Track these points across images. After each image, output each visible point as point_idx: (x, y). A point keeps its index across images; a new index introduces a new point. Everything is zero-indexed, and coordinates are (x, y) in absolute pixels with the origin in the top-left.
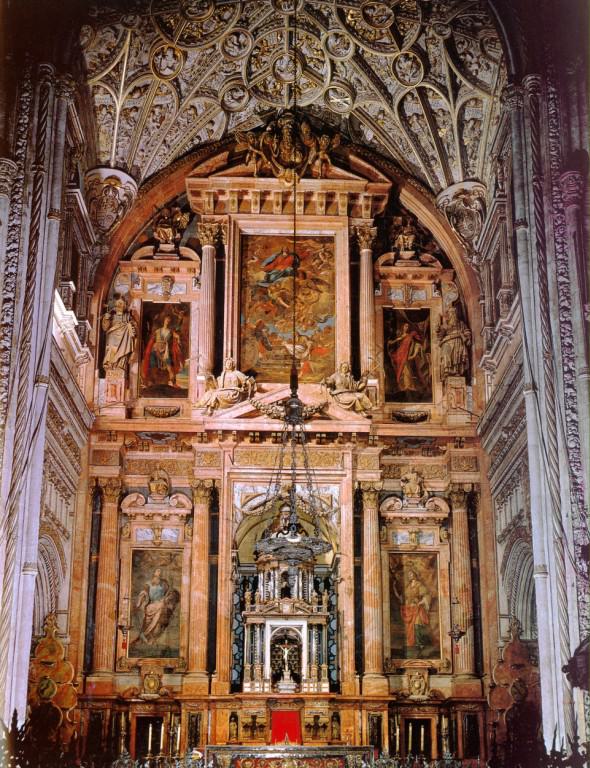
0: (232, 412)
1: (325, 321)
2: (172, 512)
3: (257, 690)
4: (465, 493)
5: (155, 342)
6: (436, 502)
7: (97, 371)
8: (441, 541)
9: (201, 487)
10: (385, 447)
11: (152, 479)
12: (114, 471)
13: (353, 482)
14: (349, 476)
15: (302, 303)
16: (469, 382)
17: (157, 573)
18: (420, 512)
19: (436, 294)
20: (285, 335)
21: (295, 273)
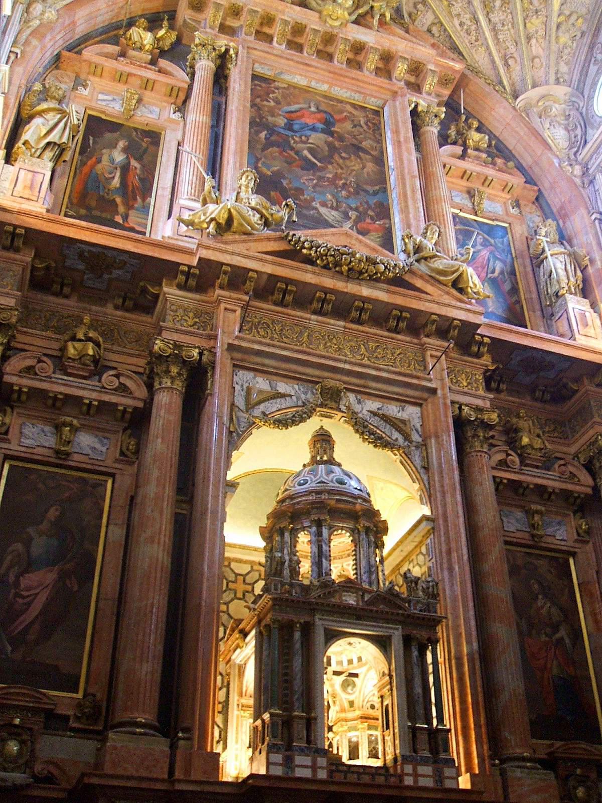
0: (252, 244)
2: (106, 398)
3: (300, 773)
5: (99, 161)
6: (571, 468)
8: (578, 534)
9: (177, 356)
11: (74, 339)
15: (338, 164)
17: (53, 513)
18: (551, 481)
19: (514, 211)
20: (316, 196)
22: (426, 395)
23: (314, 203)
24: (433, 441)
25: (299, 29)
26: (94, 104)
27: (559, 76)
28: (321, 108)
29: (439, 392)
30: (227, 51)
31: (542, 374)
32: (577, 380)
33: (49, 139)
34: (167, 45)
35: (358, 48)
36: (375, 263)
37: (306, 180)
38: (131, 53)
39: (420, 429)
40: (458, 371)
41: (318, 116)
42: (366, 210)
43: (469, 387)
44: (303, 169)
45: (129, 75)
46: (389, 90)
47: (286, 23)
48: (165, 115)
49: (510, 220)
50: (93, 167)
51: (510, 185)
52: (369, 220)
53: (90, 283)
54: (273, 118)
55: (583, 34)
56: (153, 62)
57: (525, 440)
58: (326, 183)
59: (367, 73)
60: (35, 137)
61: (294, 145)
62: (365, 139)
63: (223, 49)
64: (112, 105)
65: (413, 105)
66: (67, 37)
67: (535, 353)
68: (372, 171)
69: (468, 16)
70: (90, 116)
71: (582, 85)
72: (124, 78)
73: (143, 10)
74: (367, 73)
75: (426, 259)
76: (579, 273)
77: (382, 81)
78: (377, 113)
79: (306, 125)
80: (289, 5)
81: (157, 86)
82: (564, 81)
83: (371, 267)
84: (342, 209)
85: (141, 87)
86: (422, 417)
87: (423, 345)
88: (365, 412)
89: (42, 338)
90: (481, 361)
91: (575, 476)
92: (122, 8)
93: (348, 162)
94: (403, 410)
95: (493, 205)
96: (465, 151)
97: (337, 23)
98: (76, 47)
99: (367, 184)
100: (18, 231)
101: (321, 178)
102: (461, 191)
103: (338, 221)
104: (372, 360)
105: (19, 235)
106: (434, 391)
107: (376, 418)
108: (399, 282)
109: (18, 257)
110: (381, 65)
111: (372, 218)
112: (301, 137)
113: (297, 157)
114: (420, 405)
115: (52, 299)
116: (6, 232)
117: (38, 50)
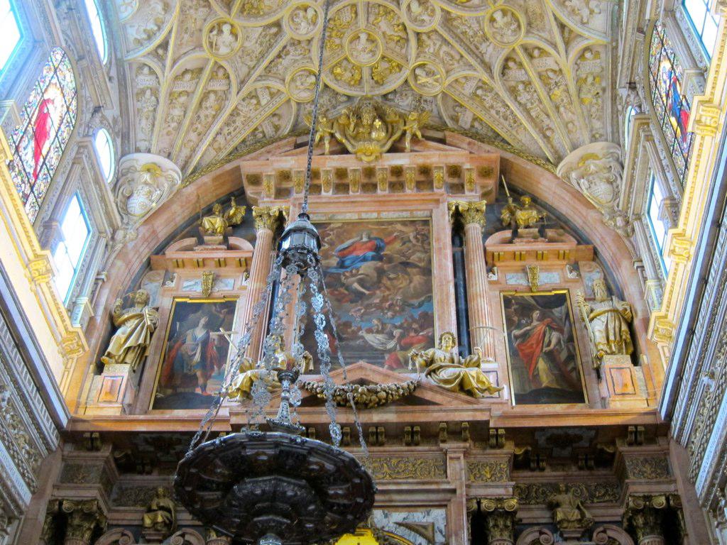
1: (420, 305)
4: (657, 511)
5: (184, 343)
6: (610, 533)
7: (92, 367)
10: (519, 452)
11: (150, 510)
12: (90, 492)
13: (469, 500)
14: (462, 491)
16: (635, 360)
20: (363, 324)
21: (380, 258)
22: (449, 496)
23: (360, 333)
24: (454, 538)
25: (341, 173)
26: (180, 293)
27: (594, 132)
28: (372, 236)
29: (458, 492)
30: (281, 213)
31: (574, 445)
32: (613, 443)
33: (128, 345)
34: (238, 219)
35: (397, 171)
36: (377, 392)
37: (355, 312)
38: (206, 238)
39: (443, 530)
40: (482, 465)
41: (369, 245)
42: (410, 325)
43: (493, 478)
44: (352, 302)
45: (204, 260)
46: (431, 200)
47: (327, 172)
48: (238, 285)
49: (567, 285)
50: (178, 350)
51: (562, 252)
52: (412, 334)
53: (163, 459)
54: (327, 261)
55: (604, 90)
56: (225, 241)
57: (560, 516)
58: (373, 309)
59: (410, 191)
60: (116, 346)
61: (345, 281)
62: (414, 253)
63: (277, 214)
64: (195, 288)
65: (454, 208)
66: (152, 245)
67: (555, 431)
68: (419, 283)
69: (500, 105)
70: (178, 304)
71: (616, 135)
72: (201, 264)
73: (217, 196)
74: (410, 191)
75: (434, 371)
76: (624, 327)
77: (426, 193)
78: (426, 223)
79: (357, 258)
80: (328, 156)
81: (228, 262)
82: (601, 136)
83: (374, 397)
84: (388, 330)
85: (216, 267)
86: (447, 518)
87: (441, 450)
88: (391, 524)
89: (131, 512)
90: (505, 450)
91: (615, 540)
92: (197, 202)
93: (395, 282)
94: (428, 514)
95: (550, 275)
96: (515, 234)
97: (372, 158)
98: (160, 250)
99: (413, 297)
100: (93, 436)
101: (367, 307)
102: (517, 271)
103: (383, 344)
104: (394, 476)
105: (96, 438)
106: (454, 491)
107: (402, 528)
108: (410, 398)
109: (99, 454)
110: (422, 178)
111: (416, 331)
112: (351, 272)
113: (346, 292)
114: (446, 506)
115: (139, 477)
116: (86, 438)
117: (124, 267)
